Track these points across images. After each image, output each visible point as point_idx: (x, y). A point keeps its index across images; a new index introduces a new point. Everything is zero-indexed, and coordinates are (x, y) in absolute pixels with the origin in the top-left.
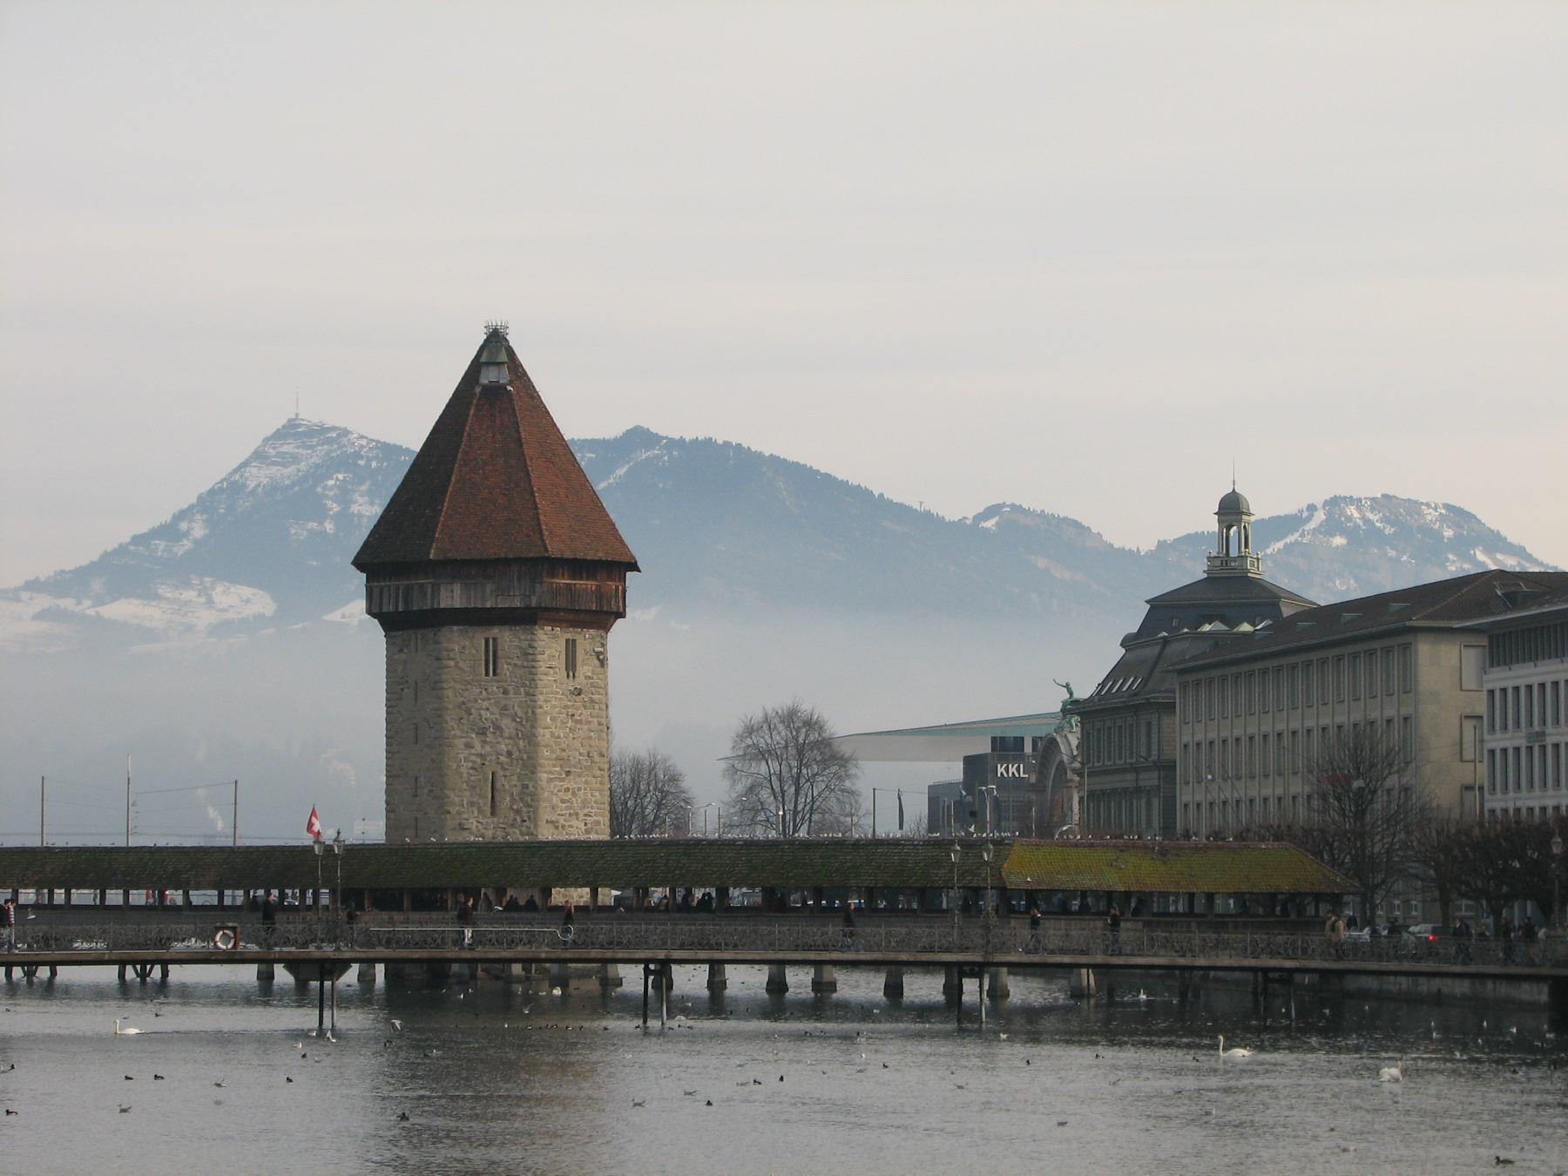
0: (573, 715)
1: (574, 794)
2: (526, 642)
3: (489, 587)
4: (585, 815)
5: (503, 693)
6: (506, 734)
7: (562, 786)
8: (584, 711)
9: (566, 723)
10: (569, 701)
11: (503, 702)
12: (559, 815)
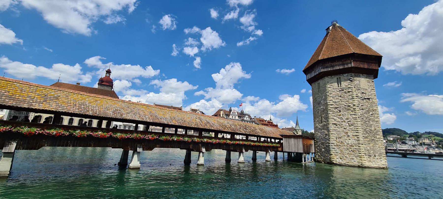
0: (341, 96)
2: (324, 81)
5: (322, 94)
8: (346, 94)
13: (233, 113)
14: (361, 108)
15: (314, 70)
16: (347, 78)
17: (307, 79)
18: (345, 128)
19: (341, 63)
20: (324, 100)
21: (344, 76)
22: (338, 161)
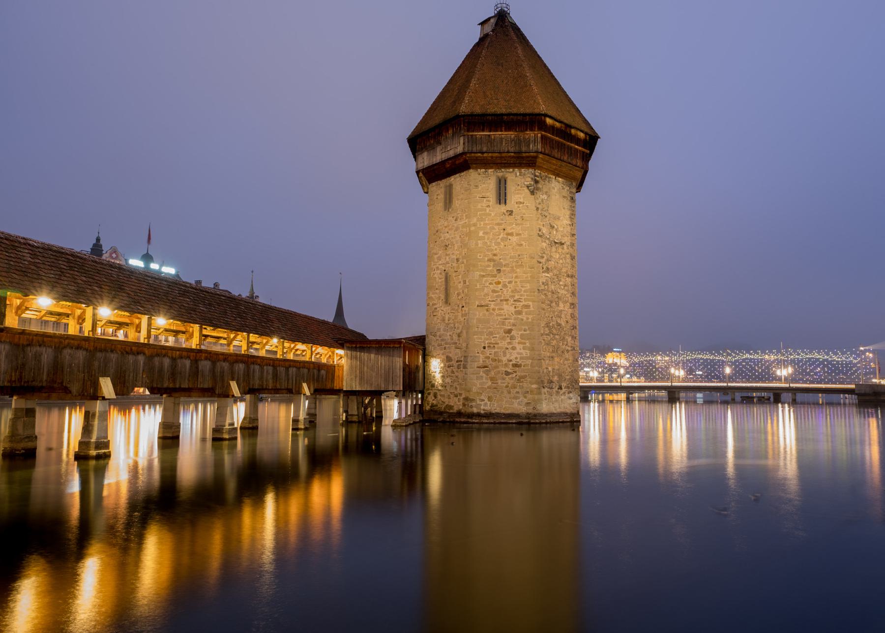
1: (505, 286)
3: (439, 149)
4: (515, 301)
6: (456, 248)
7: (492, 280)
9: (499, 235)
10: (502, 220)
11: (455, 225)
12: (489, 301)
14: (545, 267)
15: (441, 144)
16: (523, 181)
17: (419, 169)
18: (505, 319)
20: (460, 237)
21: (516, 174)
22: (482, 407)
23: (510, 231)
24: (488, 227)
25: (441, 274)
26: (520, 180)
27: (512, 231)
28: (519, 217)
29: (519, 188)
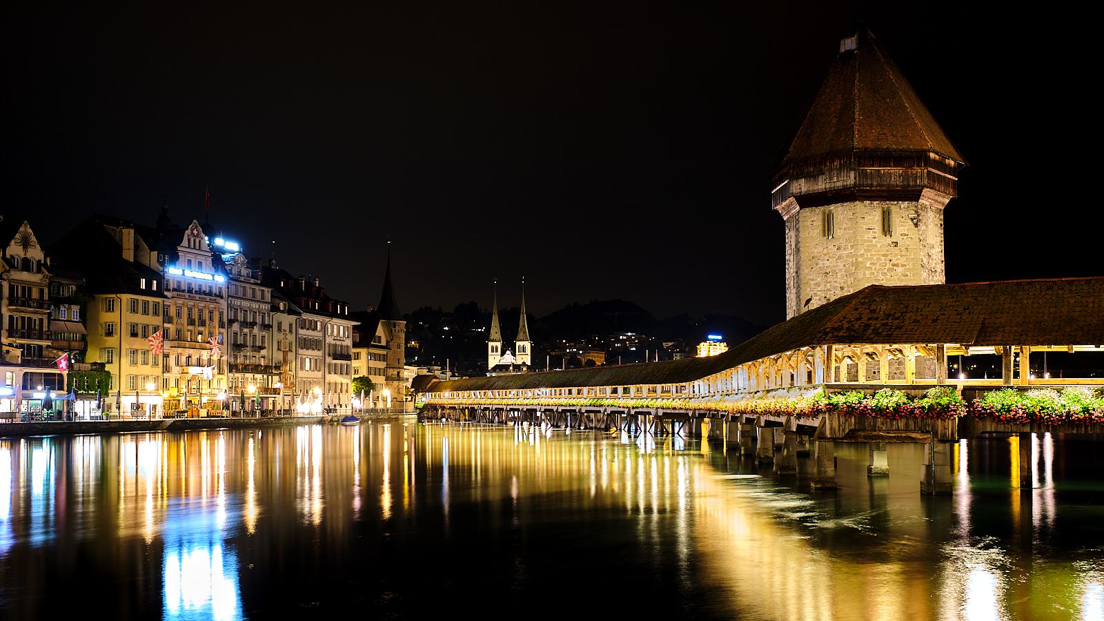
6: (839, 275)
10: (888, 251)
13: (189, 240)
16: (907, 213)
19: (901, 172)
23: (896, 263)
24: (875, 258)
25: (819, 300)
26: (905, 213)
27: (898, 262)
28: (903, 249)
29: (903, 220)
